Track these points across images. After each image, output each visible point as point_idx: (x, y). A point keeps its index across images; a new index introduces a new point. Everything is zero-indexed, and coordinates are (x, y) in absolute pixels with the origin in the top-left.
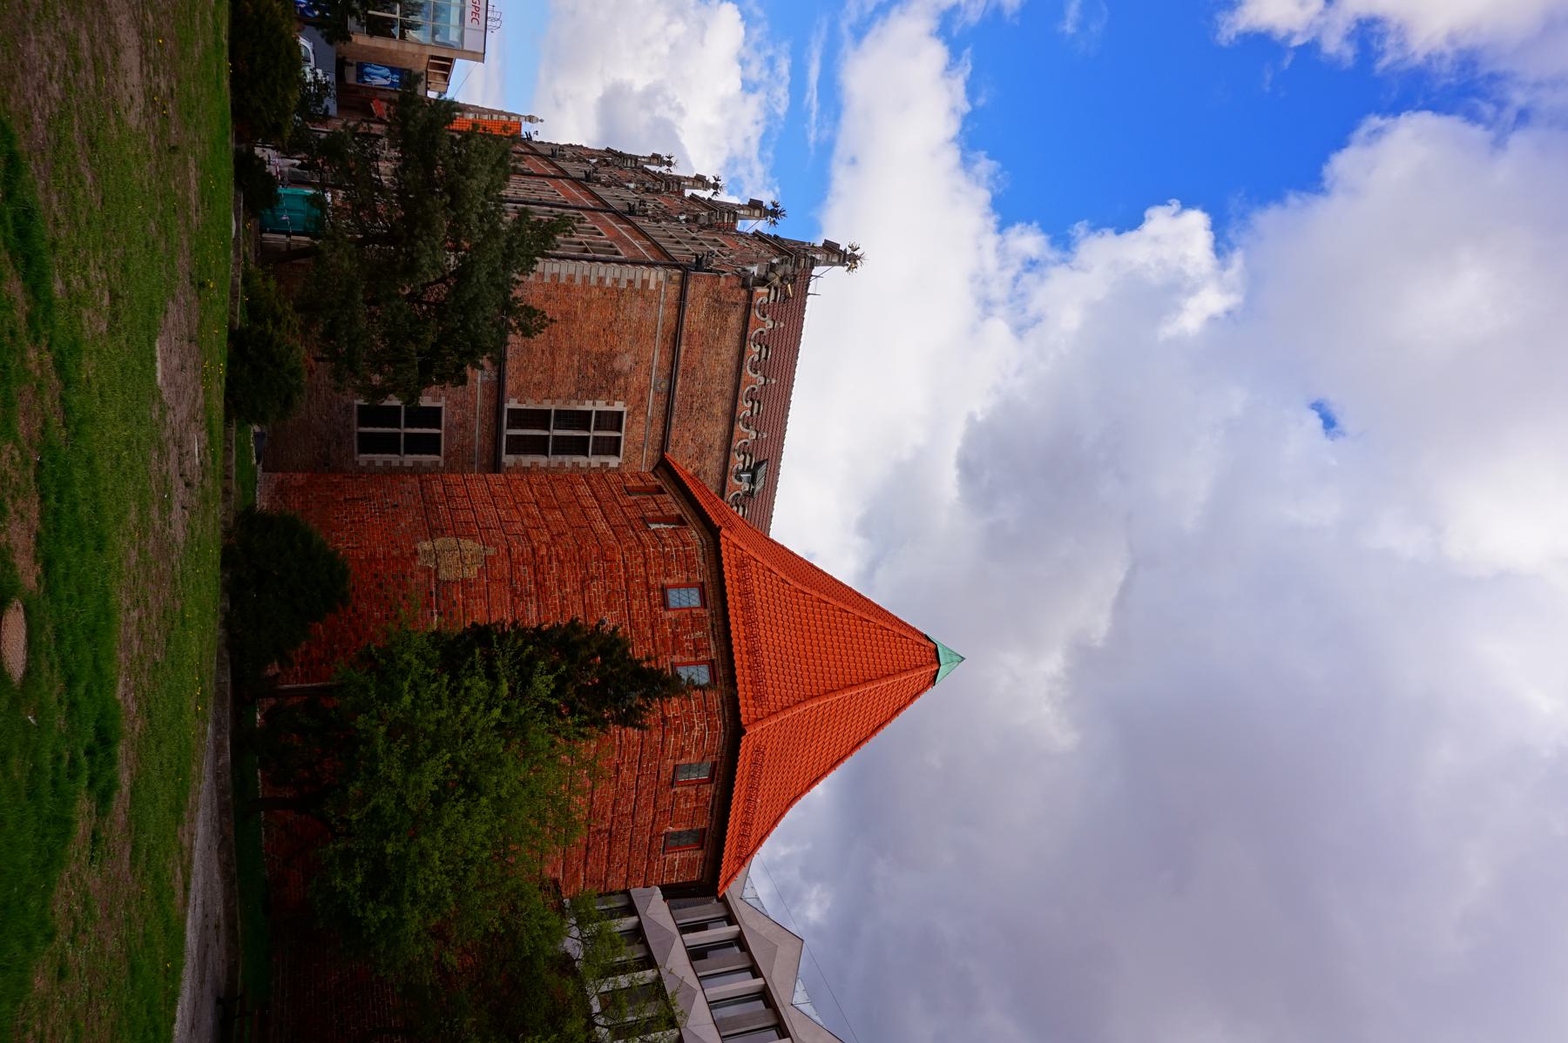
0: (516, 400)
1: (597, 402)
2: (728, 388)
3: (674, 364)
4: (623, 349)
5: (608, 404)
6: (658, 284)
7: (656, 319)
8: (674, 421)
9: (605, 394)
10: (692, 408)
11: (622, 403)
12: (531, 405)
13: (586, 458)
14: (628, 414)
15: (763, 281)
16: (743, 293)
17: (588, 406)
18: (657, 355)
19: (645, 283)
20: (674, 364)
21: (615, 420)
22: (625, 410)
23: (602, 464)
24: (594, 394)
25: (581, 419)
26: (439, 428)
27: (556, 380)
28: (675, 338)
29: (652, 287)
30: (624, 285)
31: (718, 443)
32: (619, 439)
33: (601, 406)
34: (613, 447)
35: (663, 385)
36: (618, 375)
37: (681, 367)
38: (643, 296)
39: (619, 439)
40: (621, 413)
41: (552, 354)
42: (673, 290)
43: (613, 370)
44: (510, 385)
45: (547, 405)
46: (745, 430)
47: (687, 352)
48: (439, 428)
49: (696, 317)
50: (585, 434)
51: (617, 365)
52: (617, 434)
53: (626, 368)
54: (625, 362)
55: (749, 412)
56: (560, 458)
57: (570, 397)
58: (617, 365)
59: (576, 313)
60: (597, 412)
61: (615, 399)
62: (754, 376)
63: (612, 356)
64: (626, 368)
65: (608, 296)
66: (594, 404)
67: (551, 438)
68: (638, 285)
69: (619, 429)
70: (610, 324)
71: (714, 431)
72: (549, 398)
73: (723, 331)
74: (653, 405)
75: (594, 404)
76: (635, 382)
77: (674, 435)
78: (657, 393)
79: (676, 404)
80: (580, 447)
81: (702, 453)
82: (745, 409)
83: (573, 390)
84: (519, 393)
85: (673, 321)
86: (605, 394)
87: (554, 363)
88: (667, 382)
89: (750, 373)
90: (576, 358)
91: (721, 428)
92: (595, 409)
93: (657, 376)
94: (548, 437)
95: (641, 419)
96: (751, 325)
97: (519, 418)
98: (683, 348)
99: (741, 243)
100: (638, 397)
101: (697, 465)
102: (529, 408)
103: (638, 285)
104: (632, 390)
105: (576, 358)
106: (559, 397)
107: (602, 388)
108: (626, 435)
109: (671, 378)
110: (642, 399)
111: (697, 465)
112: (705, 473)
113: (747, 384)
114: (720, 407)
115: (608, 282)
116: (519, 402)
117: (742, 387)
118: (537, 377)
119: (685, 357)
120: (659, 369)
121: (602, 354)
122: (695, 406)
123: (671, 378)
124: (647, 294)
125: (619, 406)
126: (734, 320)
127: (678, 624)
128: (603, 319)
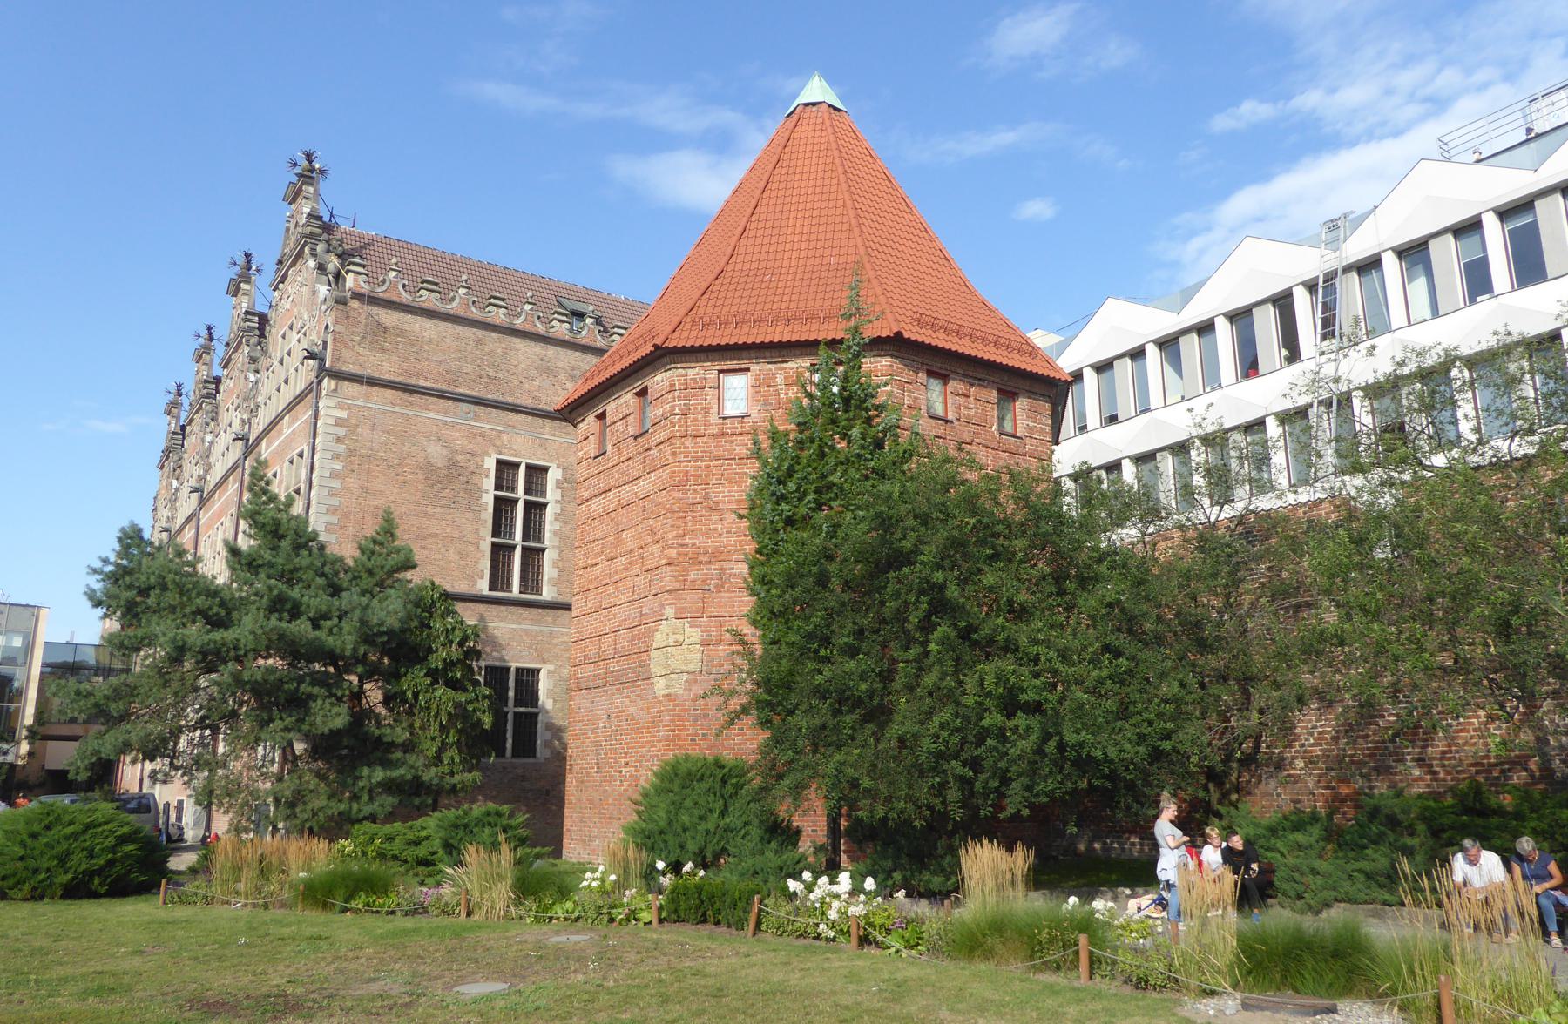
0: (479, 581)
3: (441, 395)
5: (487, 476)
6: (340, 406)
7: (385, 412)
8: (510, 400)
9: (475, 478)
11: (487, 459)
12: (486, 564)
13: (549, 507)
14: (500, 453)
17: (489, 499)
18: (431, 414)
19: (338, 422)
20: (441, 395)
21: (505, 469)
22: (495, 456)
23: (557, 487)
24: (475, 492)
25: (503, 507)
27: (456, 534)
29: (343, 414)
30: (341, 448)
32: (529, 467)
33: (489, 483)
34: (537, 473)
36: (453, 462)
39: (529, 467)
40: (499, 462)
41: (425, 538)
42: (349, 388)
43: (447, 468)
45: (486, 547)
50: (520, 507)
51: (440, 463)
52: (522, 471)
53: (445, 452)
54: (436, 453)
55: (502, 311)
56: (547, 535)
57: (477, 519)
58: (440, 463)
59: (377, 507)
61: (482, 467)
63: (428, 468)
64: (445, 452)
66: (487, 492)
67: (526, 544)
68: (342, 431)
69: (517, 465)
70: (390, 467)
73: (401, 332)
74: (491, 422)
75: (487, 492)
76: (461, 442)
77: (527, 401)
79: (489, 397)
80: (535, 510)
81: (548, 371)
83: (470, 515)
86: (475, 478)
87: (437, 535)
88: (461, 404)
89: (454, 304)
90: (430, 510)
91: (519, 343)
93: (456, 416)
94: (523, 548)
95: (505, 438)
96: (394, 298)
97: (499, 577)
98: (422, 383)
99: (288, 305)
100: (480, 439)
101: (562, 377)
103: (342, 431)
104: (471, 446)
106: (477, 532)
108: (524, 457)
110: (482, 435)
111: (562, 377)
112: (573, 369)
115: (338, 466)
116: (482, 578)
117: (471, 316)
118: (452, 555)
119: (433, 381)
120: (446, 413)
122: (492, 373)
124: (354, 421)
125: (490, 464)
126: (389, 317)
127: (766, 403)
128: (384, 475)
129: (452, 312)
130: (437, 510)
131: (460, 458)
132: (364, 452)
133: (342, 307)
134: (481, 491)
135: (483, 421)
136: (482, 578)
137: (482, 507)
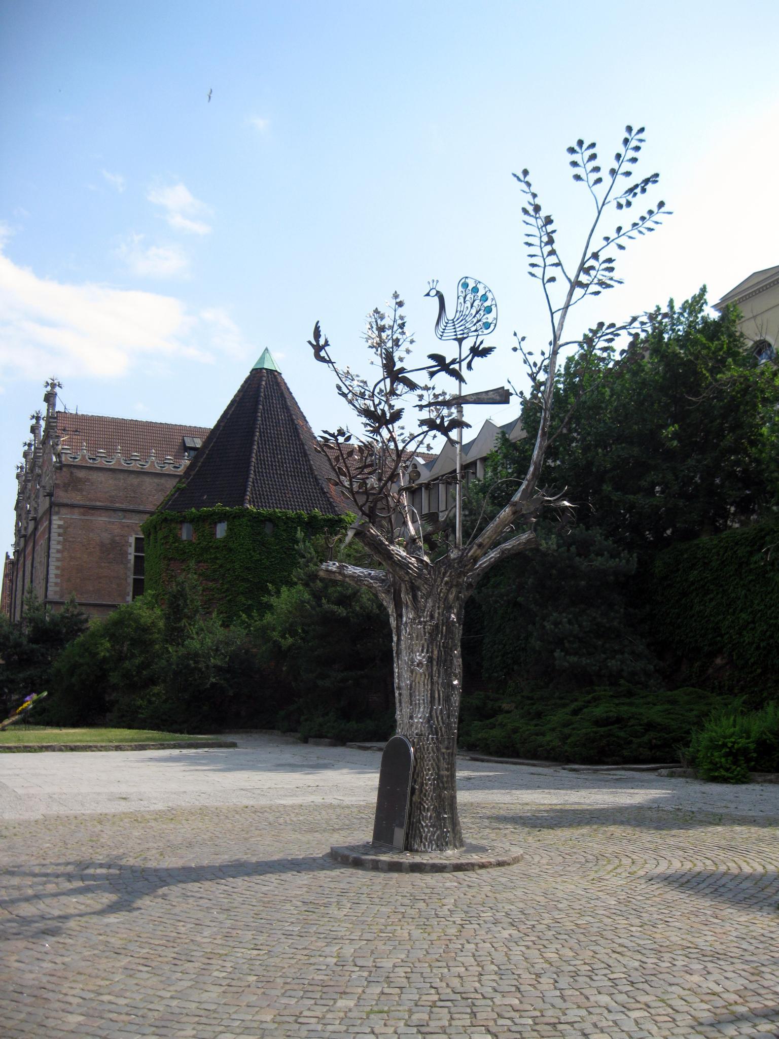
1: (129, 552)
2: (121, 476)
3: (106, 509)
5: (130, 546)
6: (60, 519)
7: (80, 520)
10: (134, 497)
12: (130, 589)
16: (64, 469)
17: (131, 558)
18: (101, 519)
19: (60, 527)
20: (106, 509)
22: (134, 536)
29: (61, 523)
30: (61, 538)
31: (156, 480)
33: (132, 550)
35: (120, 514)
37: (109, 504)
38: (67, 528)
40: (136, 539)
42: (64, 511)
47: (100, 501)
49: (76, 498)
54: (106, 537)
60: (136, 551)
61: (128, 542)
63: (102, 545)
64: (109, 536)
65: (67, 547)
66: (130, 554)
68: (61, 531)
72: (126, 579)
75: (130, 554)
78: (125, 517)
84: (123, 596)
85: (82, 510)
90: (103, 564)
91: (147, 480)
98: (98, 504)
102: (132, 589)
103: (61, 531)
106: (126, 574)
109: (115, 510)
110: (128, 526)
113: (120, 464)
114: (134, 480)
115: (59, 547)
120: (110, 517)
123: (115, 510)
125: (132, 540)
126: (81, 474)
129: (112, 467)
130: (107, 564)
132: (71, 539)
133: (58, 471)
134: (127, 553)
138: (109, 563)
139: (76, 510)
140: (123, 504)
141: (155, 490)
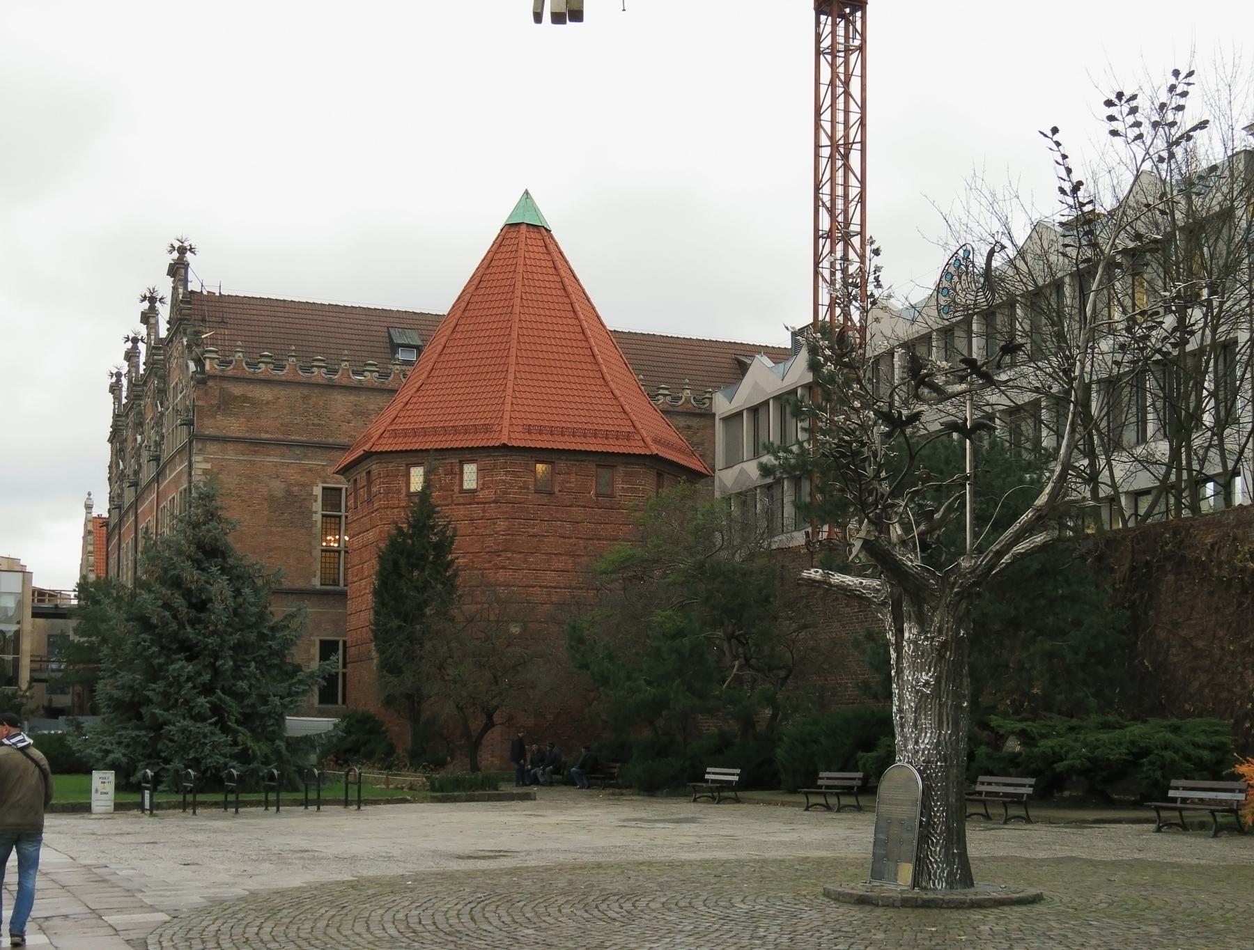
3: (277, 443)
4: (266, 489)
5: (316, 501)
6: (206, 460)
7: (238, 461)
8: (331, 440)
10: (319, 425)
11: (315, 488)
14: (325, 482)
15: (199, 362)
16: (210, 383)
17: (318, 517)
18: (272, 459)
19: (205, 472)
20: (277, 443)
22: (321, 485)
26: (337, 642)
28: (255, 444)
29: (208, 466)
31: (352, 398)
33: (318, 506)
36: (289, 493)
37: (280, 437)
40: (324, 488)
41: (271, 550)
42: (212, 448)
44: (300, 584)
46: (340, 373)
47: (267, 432)
48: (337, 642)
49: (233, 426)
51: (279, 494)
53: (283, 486)
54: (277, 486)
58: (279, 494)
61: (311, 494)
62: (287, 367)
63: (271, 499)
64: (283, 486)
66: (316, 512)
70: (243, 501)
71: (341, 403)
75: (316, 512)
78: (306, 457)
81: (362, 413)
82: (319, 374)
83: (303, 531)
85: (240, 447)
90: (273, 529)
92: (320, 512)
96: (239, 374)
98: (264, 436)
100: (308, 473)
105: (273, 529)
106: (310, 543)
107: (301, 507)
109: (291, 445)
110: (310, 470)
116: (315, 576)
117: (298, 379)
120: (283, 456)
121: (270, 507)
122: (316, 422)
123: (291, 445)
124: (215, 470)
125: (318, 491)
126: (237, 390)
129: (284, 378)
130: (279, 529)
131: (295, 489)
133: (202, 386)
135: (310, 459)
136: (315, 576)
137: (313, 524)
138: (283, 527)
139: (230, 447)
140: (301, 435)
141: (352, 413)
